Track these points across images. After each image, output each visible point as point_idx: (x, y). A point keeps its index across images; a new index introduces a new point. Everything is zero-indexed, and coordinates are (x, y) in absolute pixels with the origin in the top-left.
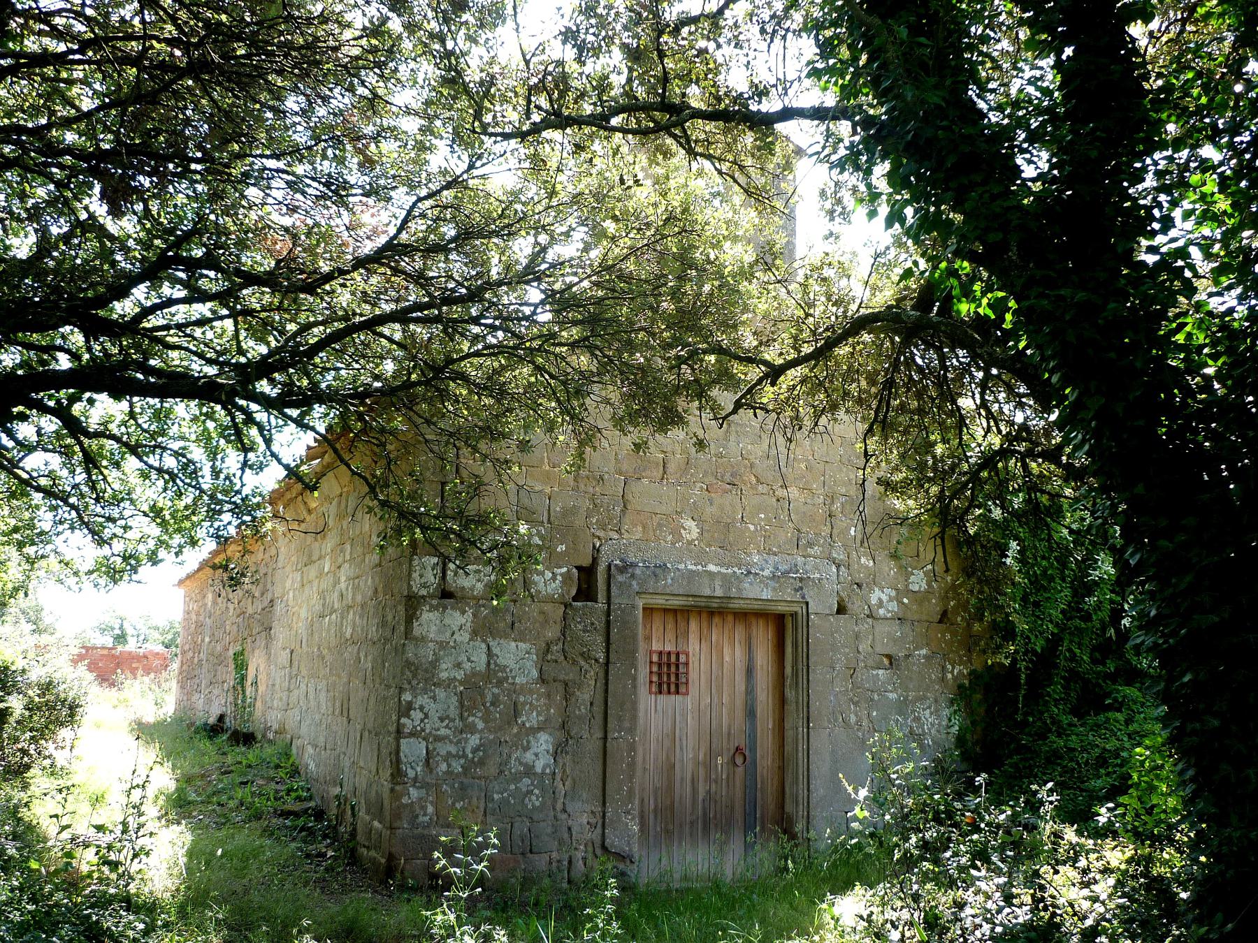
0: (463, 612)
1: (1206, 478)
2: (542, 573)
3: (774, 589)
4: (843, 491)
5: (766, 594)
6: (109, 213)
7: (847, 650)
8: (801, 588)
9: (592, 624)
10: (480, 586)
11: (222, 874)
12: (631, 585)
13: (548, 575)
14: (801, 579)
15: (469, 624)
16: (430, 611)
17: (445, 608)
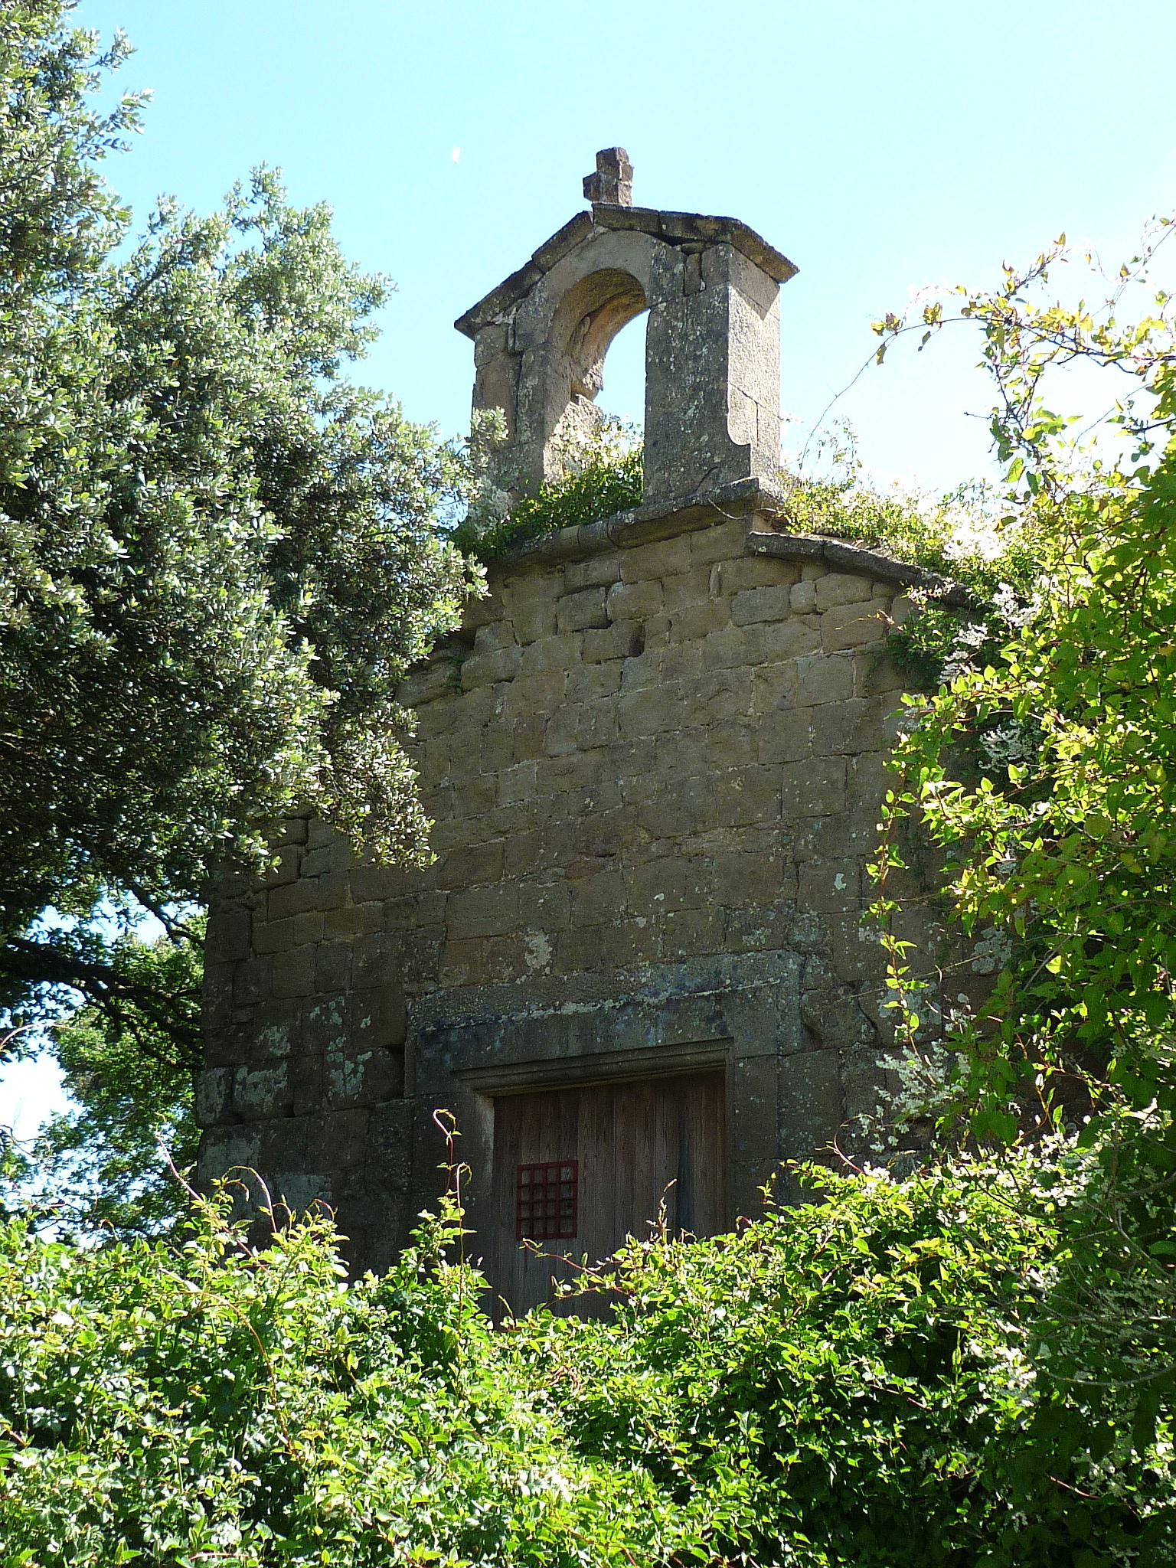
0: (250, 1140)
1: (105, 987)
2: (340, 1067)
3: (669, 1026)
4: (819, 807)
5: (656, 1038)
6: (278, 740)
7: (819, 1120)
8: (719, 1014)
9: (396, 1133)
10: (269, 1098)
11: (274, 1357)
12: (442, 1062)
13: (349, 1066)
14: (719, 998)
15: (256, 1157)
16: (214, 1145)
17: (230, 1138)
